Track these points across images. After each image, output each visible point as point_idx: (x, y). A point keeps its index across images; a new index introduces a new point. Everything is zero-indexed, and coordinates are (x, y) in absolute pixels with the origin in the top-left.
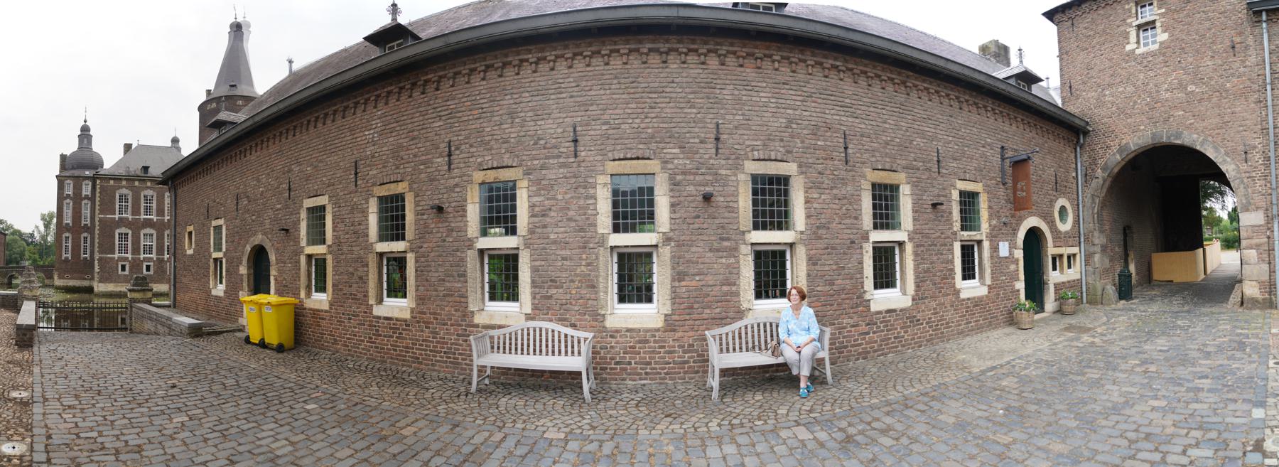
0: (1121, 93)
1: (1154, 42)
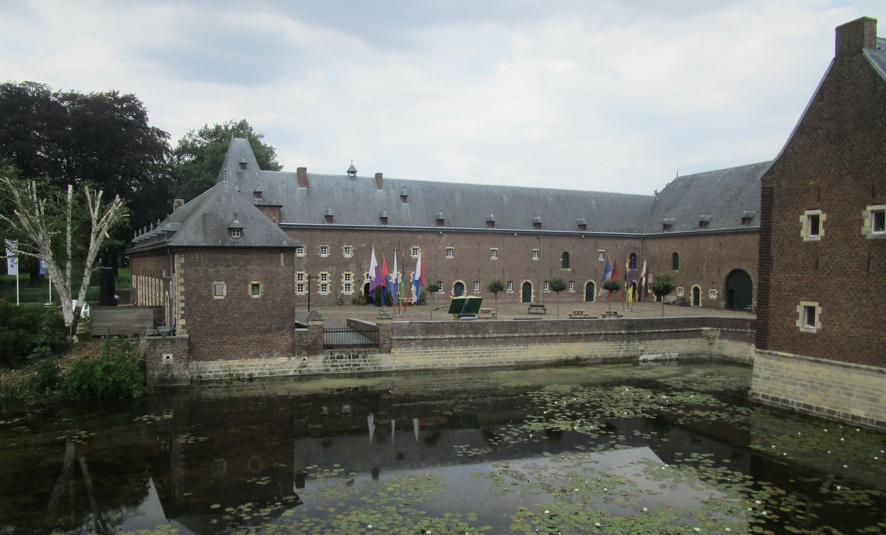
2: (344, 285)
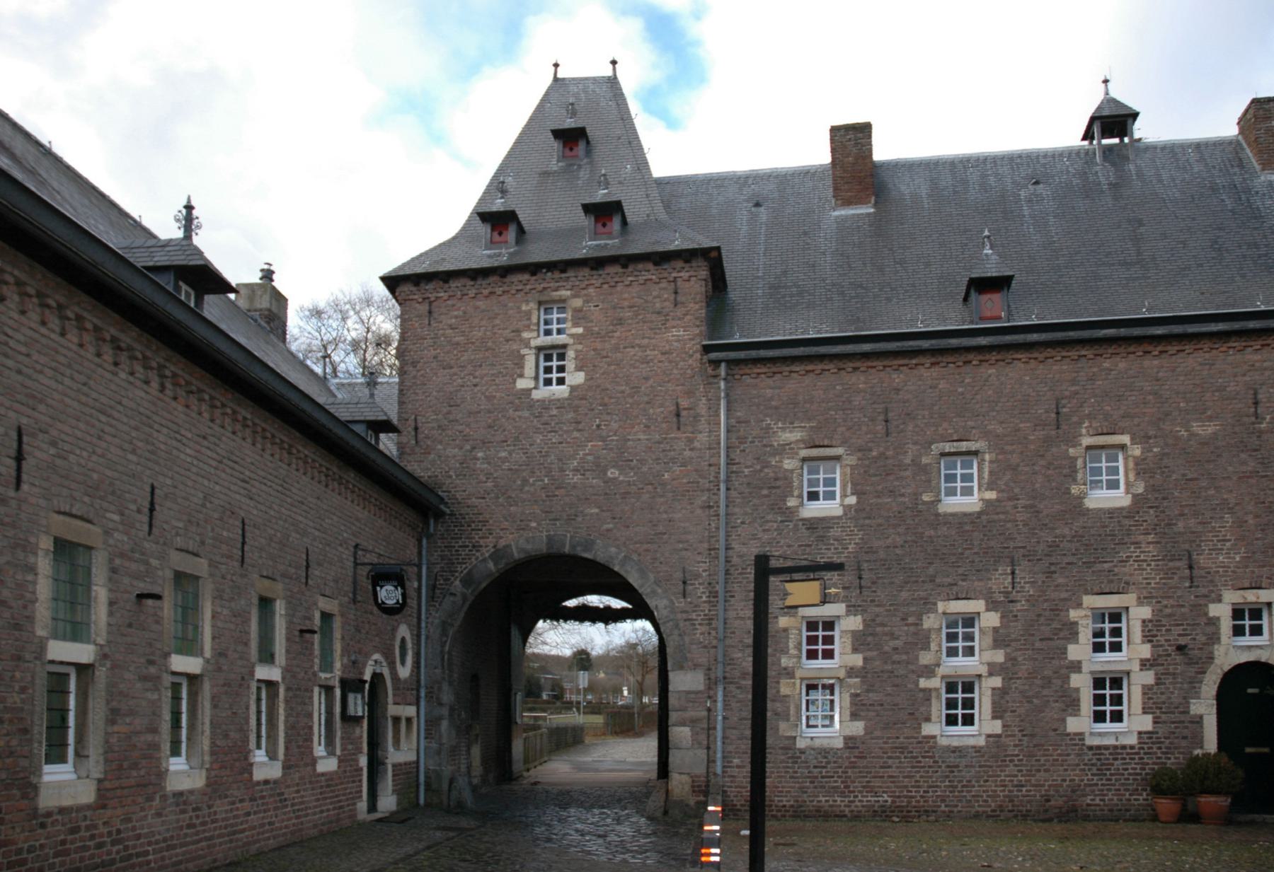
0: (504, 460)
1: (561, 381)
2: (1081, 683)
